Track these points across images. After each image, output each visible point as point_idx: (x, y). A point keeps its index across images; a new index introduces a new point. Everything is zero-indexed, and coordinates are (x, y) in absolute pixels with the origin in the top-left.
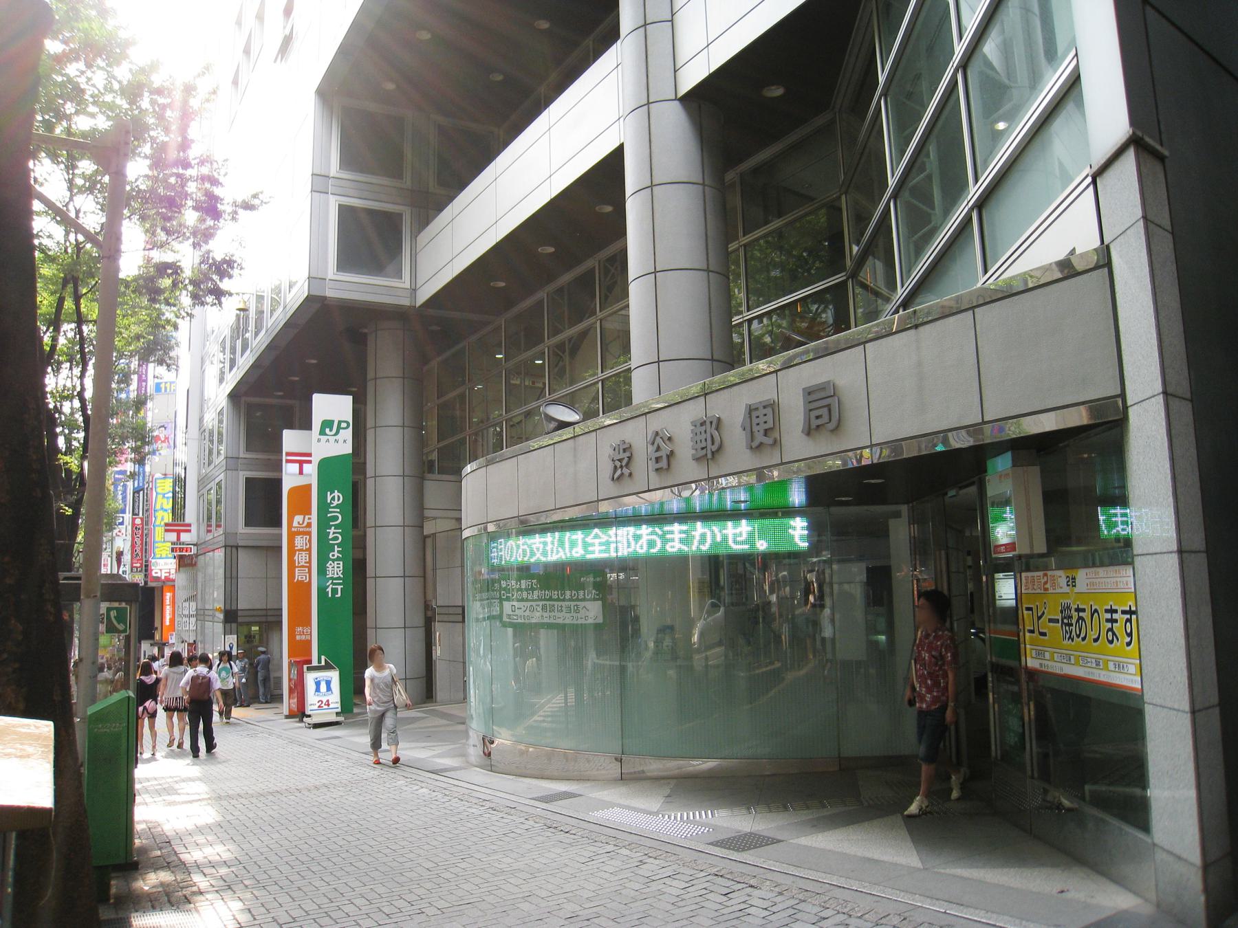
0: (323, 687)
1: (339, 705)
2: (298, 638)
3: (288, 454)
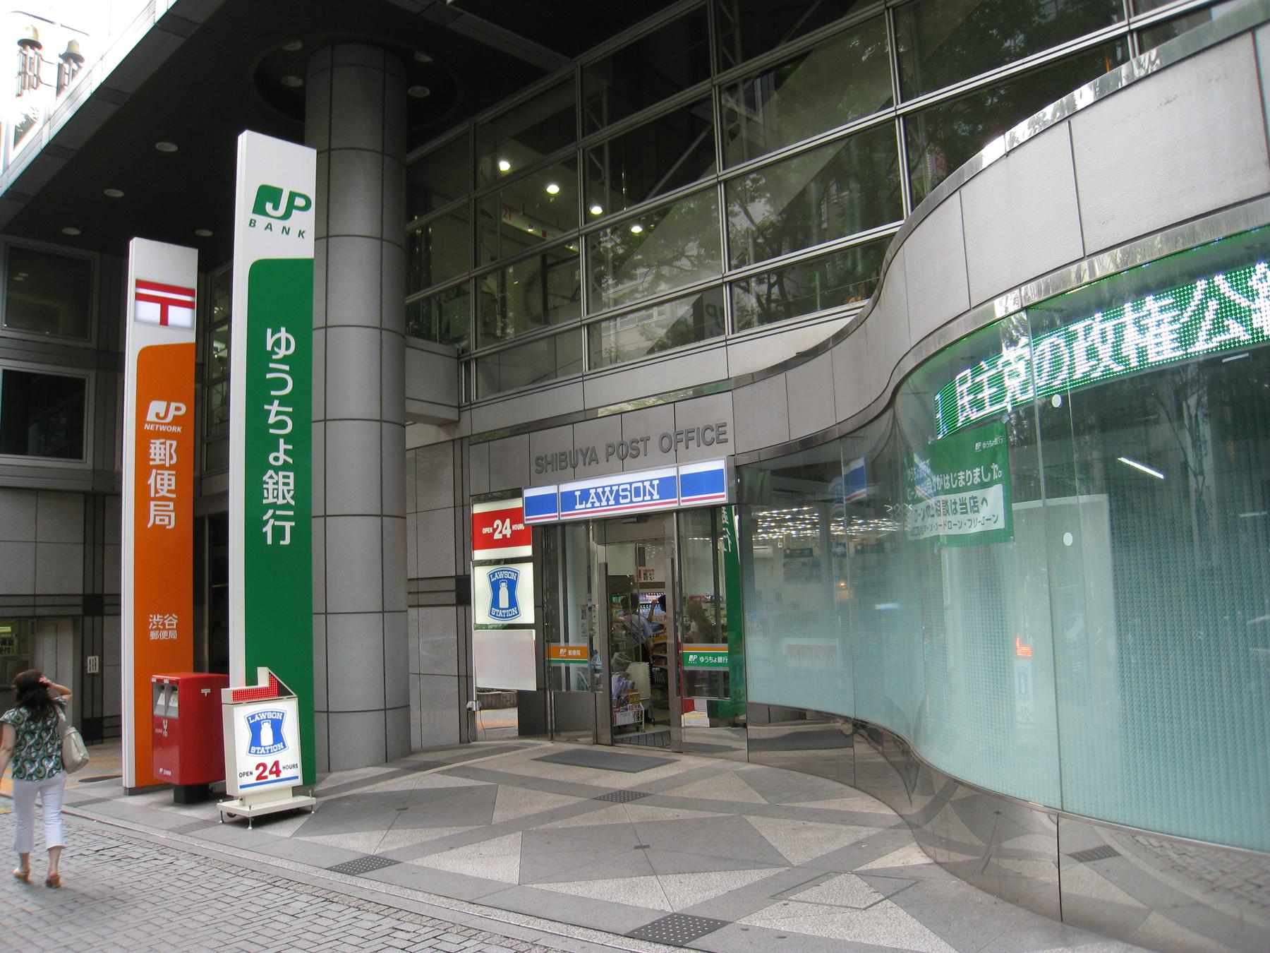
0: (267, 735)
1: (298, 772)
2: (153, 635)
3: (140, 284)
